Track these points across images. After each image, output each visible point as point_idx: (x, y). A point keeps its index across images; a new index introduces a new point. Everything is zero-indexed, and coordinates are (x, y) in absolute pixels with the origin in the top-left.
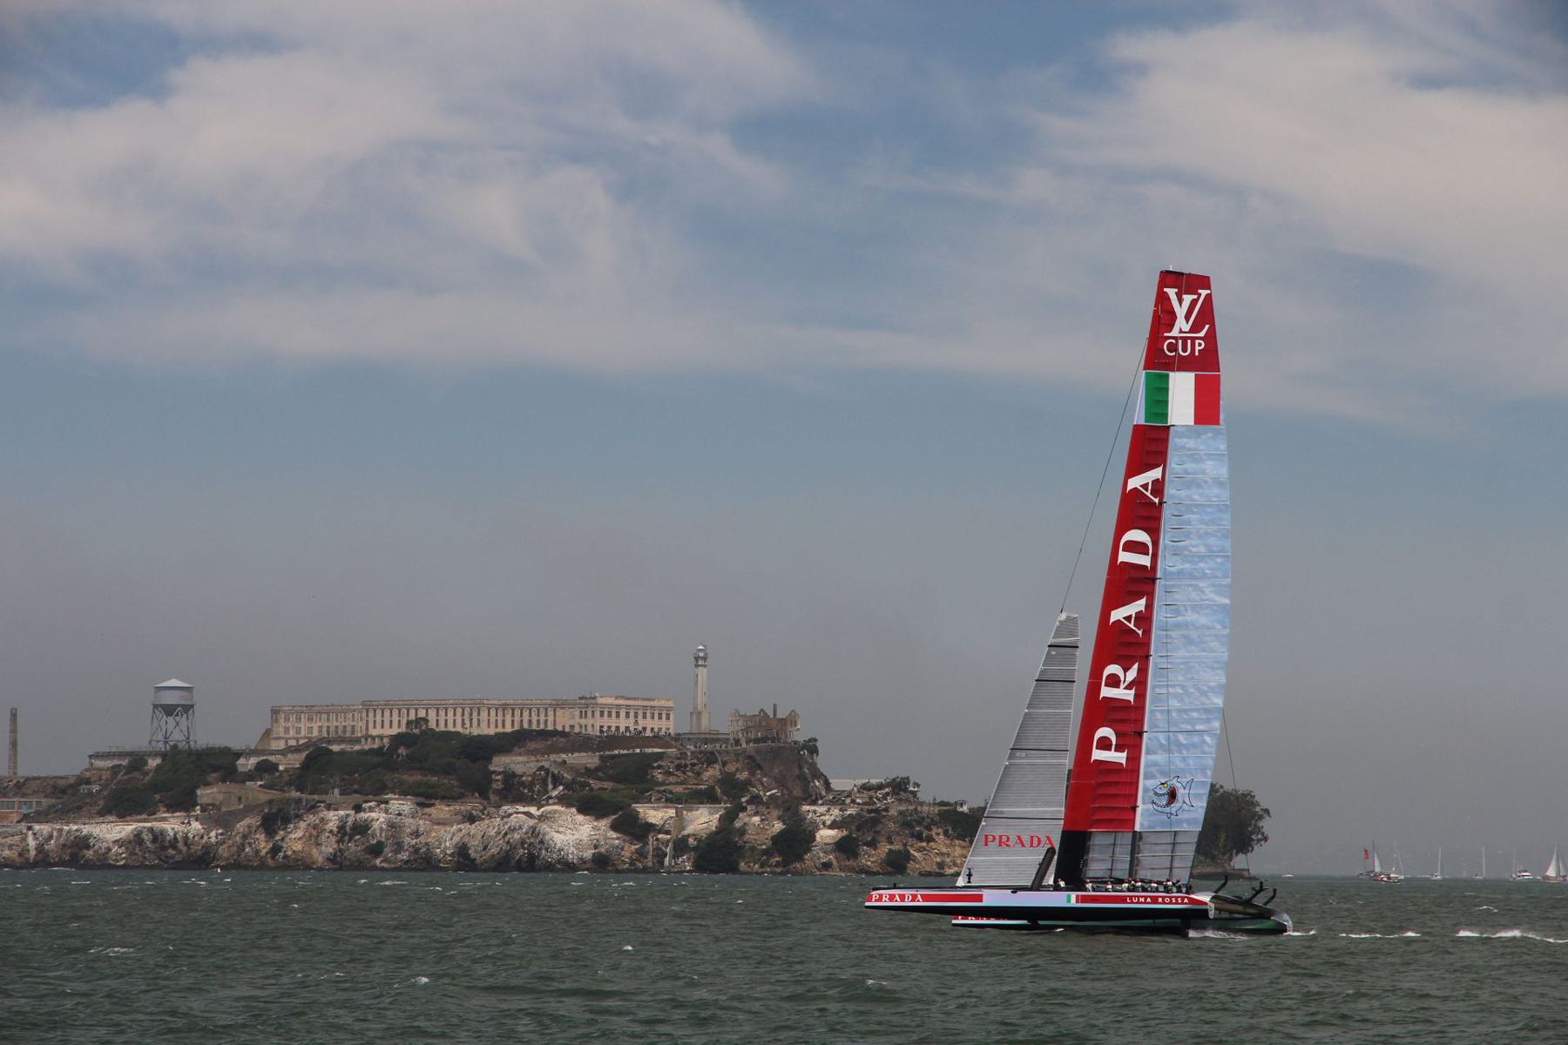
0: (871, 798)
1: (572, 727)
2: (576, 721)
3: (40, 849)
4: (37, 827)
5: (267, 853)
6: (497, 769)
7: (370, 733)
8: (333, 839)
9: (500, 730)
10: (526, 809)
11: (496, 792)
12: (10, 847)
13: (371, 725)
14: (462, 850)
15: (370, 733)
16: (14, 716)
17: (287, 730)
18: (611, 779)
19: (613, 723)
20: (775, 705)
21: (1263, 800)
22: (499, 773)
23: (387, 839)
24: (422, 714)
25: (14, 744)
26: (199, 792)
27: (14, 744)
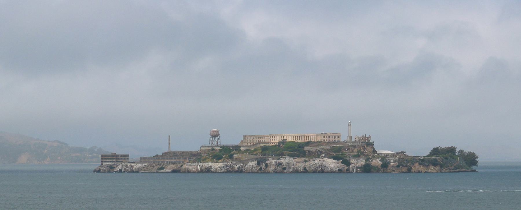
0: (400, 156)
1: (321, 140)
2: (322, 139)
3: (201, 169)
4: (200, 164)
5: (259, 169)
6: (306, 150)
7: (272, 141)
8: (274, 166)
9: (304, 141)
10: (319, 159)
11: (307, 155)
12: (194, 168)
13: (272, 140)
14: (305, 169)
15: (272, 141)
16: (169, 137)
17: (248, 141)
18: (333, 152)
19: (330, 139)
20: (365, 135)
21: (477, 154)
22: (307, 151)
23: (287, 166)
24: (285, 138)
25: (170, 144)
26: (234, 155)
27: (170, 144)
